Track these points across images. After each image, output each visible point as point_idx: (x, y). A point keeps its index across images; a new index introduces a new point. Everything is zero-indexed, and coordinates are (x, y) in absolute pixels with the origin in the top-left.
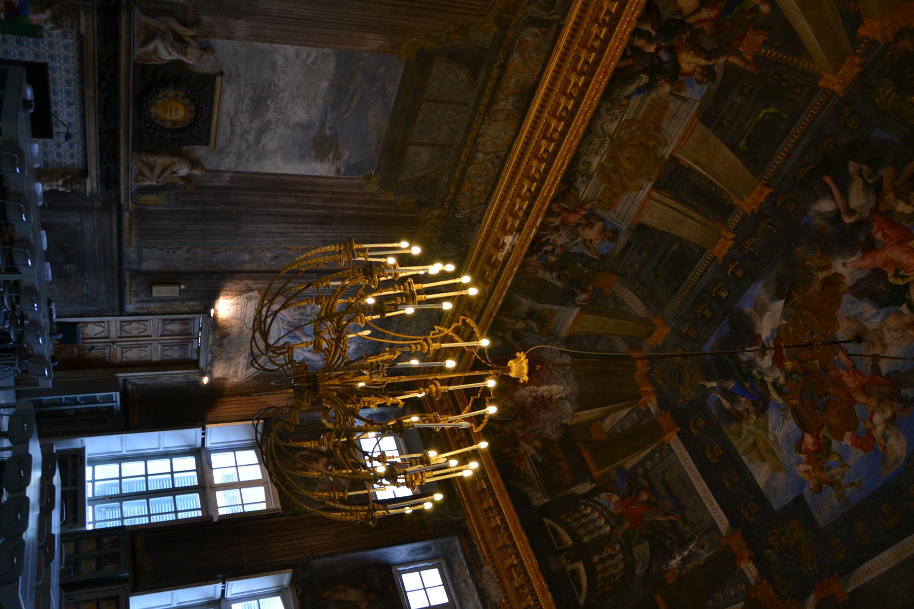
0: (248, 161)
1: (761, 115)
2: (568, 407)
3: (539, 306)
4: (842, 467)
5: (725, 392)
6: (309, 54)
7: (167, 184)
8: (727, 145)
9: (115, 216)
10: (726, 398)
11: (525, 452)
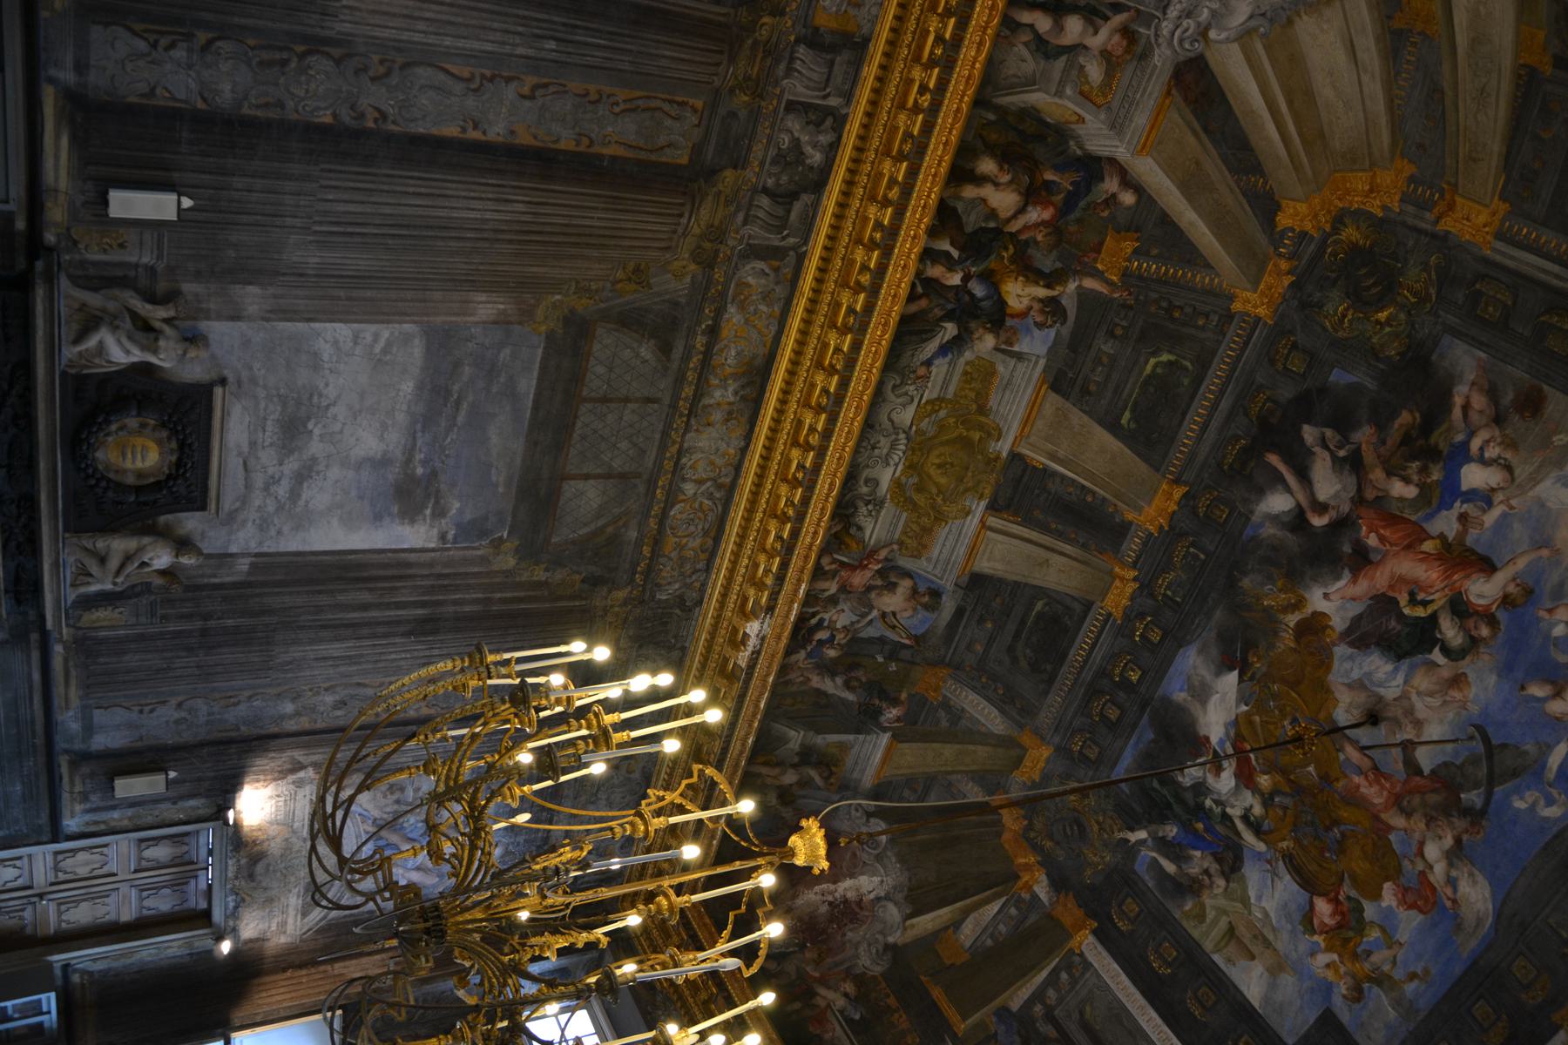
0: (279, 532)
1: (1149, 368)
2: (893, 913)
3: (820, 740)
4: (1390, 948)
5: (1163, 845)
6: (376, 337)
7: (134, 586)
8: (1100, 423)
9: (35, 656)
10: (1167, 857)
11: (829, 1006)
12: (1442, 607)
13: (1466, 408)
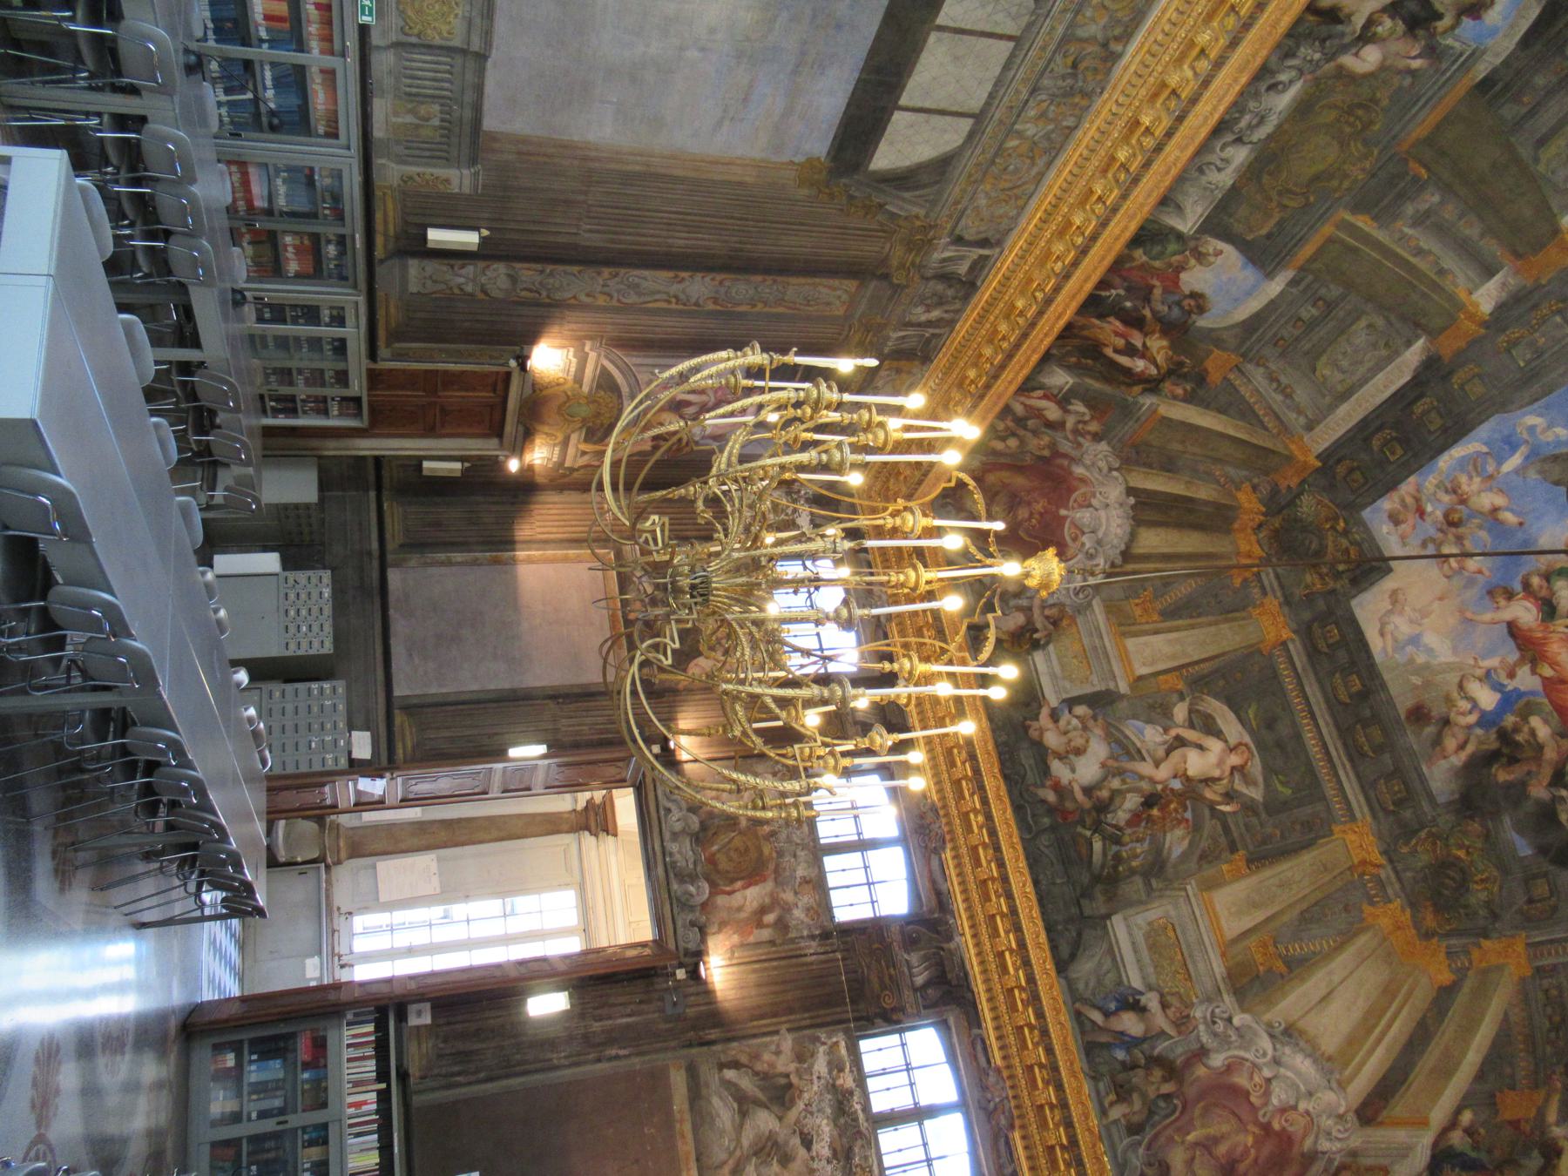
12: (1561, 617)
13: (1462, 747)
